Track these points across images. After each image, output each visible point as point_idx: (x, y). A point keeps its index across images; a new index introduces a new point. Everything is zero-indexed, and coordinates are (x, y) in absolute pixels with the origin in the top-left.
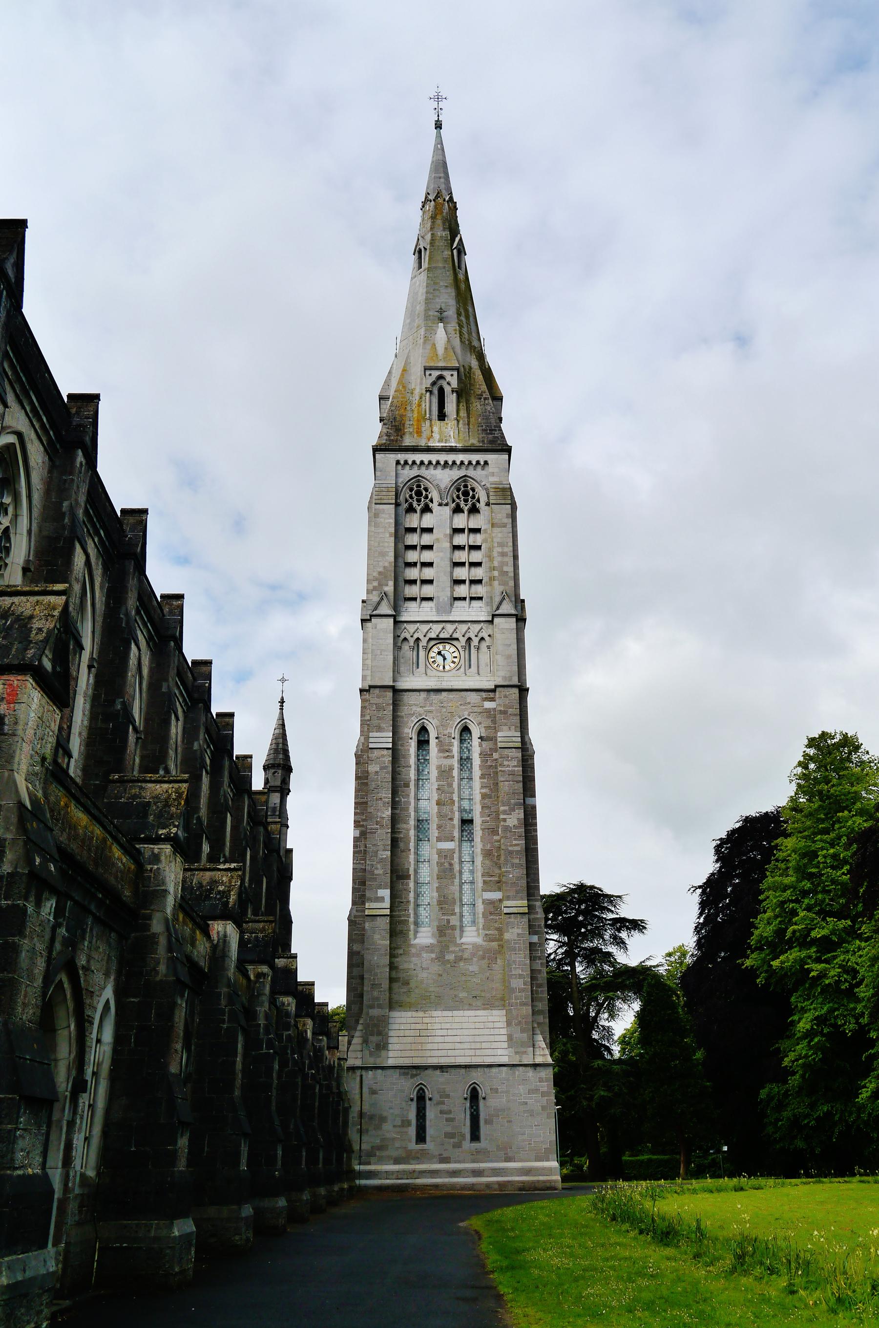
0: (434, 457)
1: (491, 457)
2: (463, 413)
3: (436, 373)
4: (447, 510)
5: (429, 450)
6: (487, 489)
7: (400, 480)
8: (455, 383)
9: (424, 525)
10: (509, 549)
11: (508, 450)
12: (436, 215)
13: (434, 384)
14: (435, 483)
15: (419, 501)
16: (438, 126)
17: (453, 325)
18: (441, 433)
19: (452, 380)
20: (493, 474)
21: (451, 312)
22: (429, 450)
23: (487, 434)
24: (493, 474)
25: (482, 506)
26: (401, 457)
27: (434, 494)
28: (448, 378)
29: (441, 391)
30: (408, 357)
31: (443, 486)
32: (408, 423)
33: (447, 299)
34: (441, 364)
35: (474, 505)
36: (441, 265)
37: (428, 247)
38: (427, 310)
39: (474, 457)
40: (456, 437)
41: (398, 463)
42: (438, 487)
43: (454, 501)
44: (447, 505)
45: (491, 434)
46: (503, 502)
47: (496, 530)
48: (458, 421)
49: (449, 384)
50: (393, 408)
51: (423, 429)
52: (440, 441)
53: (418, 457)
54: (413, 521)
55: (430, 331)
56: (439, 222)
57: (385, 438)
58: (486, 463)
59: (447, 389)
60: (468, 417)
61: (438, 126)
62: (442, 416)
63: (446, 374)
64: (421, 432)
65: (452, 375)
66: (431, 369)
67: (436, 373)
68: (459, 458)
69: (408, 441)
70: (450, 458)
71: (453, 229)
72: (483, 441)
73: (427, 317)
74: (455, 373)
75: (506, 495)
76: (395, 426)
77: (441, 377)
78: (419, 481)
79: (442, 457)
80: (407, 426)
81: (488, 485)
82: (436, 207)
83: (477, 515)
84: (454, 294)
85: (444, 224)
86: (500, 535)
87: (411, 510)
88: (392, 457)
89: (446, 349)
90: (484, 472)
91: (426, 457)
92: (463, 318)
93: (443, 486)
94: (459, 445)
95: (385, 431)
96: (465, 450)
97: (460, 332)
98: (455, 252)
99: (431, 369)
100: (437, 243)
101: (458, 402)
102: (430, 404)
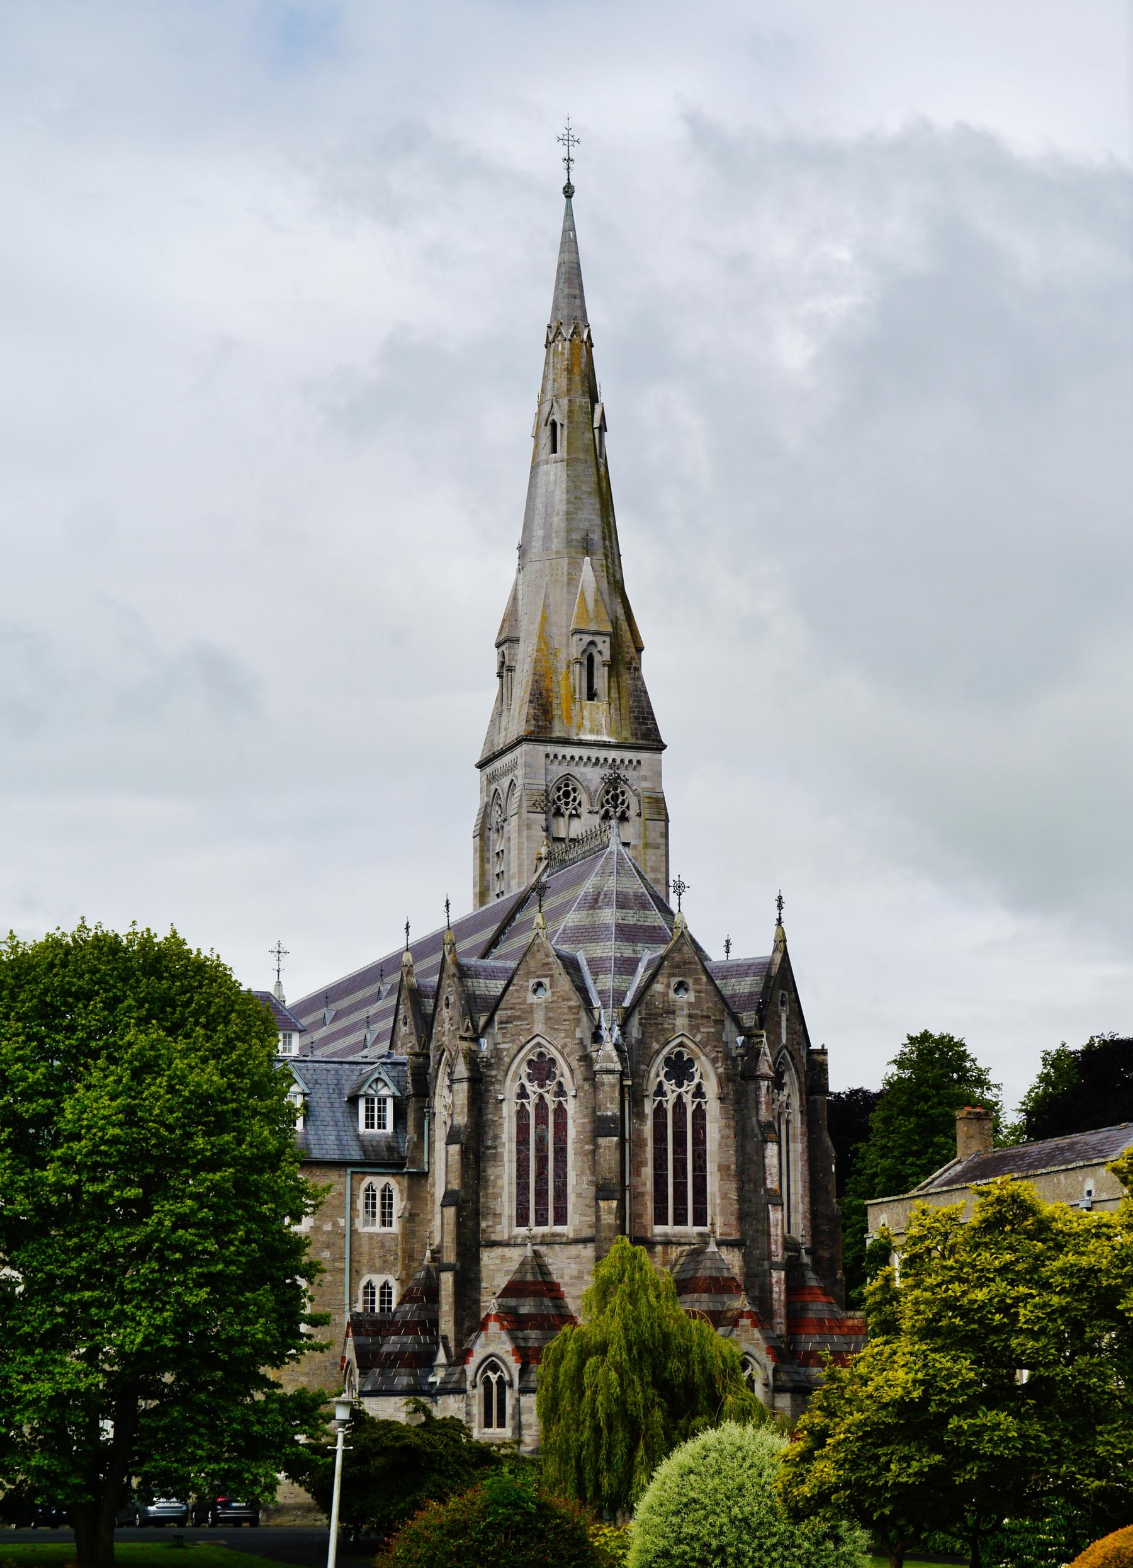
0: (584, 752)
1: (644, 756)
2: (614, 695)
3: (587, 638)
4: (597, 819)
5: (581, 743)
6: (638, 795)
7: (549, 777)
8: (607, 656)
9: (573, 835)
10: (661, 876)
11: (660, 747)
12: (573, 365)
13: (585, 651)
14: (585, 784)
15: (567, 804)
16: (568, 191)
17: (599, 556)
18: (592, 720)
19: (604, 647)
20: (645, 778)
21: (596, 537)
22: (581, 743)
23: (640, 724)
24: (645, 778)
25: (631, 813)
26: (551, 749)
27: (583, 797)
28: (600, 646)
29: (591, 659)
30: (546, 596)
31: (592, 789)
32: (555, 701)
33: (590, 515)
34: (593, 627)
35: (623, 813)
36: (582, 456)
37: (565, 423)
38: (568, 531)
39: (628, 755)
40: (608, 726)
41: (547, 756)
42: (587, 789)
43: (603, 806)
44: (597, 813)
45: (645, 724)
46: (657, 817)
47: (650, 852)
48: (610, 705)
49: (600, 652)
50: (537, 678)
51: (573, 713)
52: (592, 732)
53: (569, 751)
54: (561, 828)
55: (575, 567)
56: (577, 379)
57: (533, 722)
58: (639, 762)
59: (598, 659)
60: (620, 698)
61: (568, 191)
62: (592, 695)
63: (598, 639)
64: (571, 718)
65: (604, 642)
66: (582, 632)
67: (587, 638)
68: (612, 754)
69: (557, 733)
70: (602, 754)
71: (594, 398)
72: (636, 734)
73: (569, 542)
74: (608, 639)
75: (658, 807)
76: (542, 705)
77: (592, 643)
78: (567, 779)
79: (594, 753)
80: (554, 706)
81: (640, 790)
82: (571, 349)
83: (626, 824)
84: (598, 506)
85: (583, 385)
86: (653, 858)
87: (558, 813)
88: (542, 749)
89: (596, 601)
90: (635, 773)
91: (577, 752)
92: (607, 542)
93: (592, 789)
94: (613, 740)
95: (532, 711)
96: (618, 747)
97: (607, 567)
98: (596, 431)
99: (582, 632)
100: (576, 418)
101: (610, 676)
102: (578, 675)
